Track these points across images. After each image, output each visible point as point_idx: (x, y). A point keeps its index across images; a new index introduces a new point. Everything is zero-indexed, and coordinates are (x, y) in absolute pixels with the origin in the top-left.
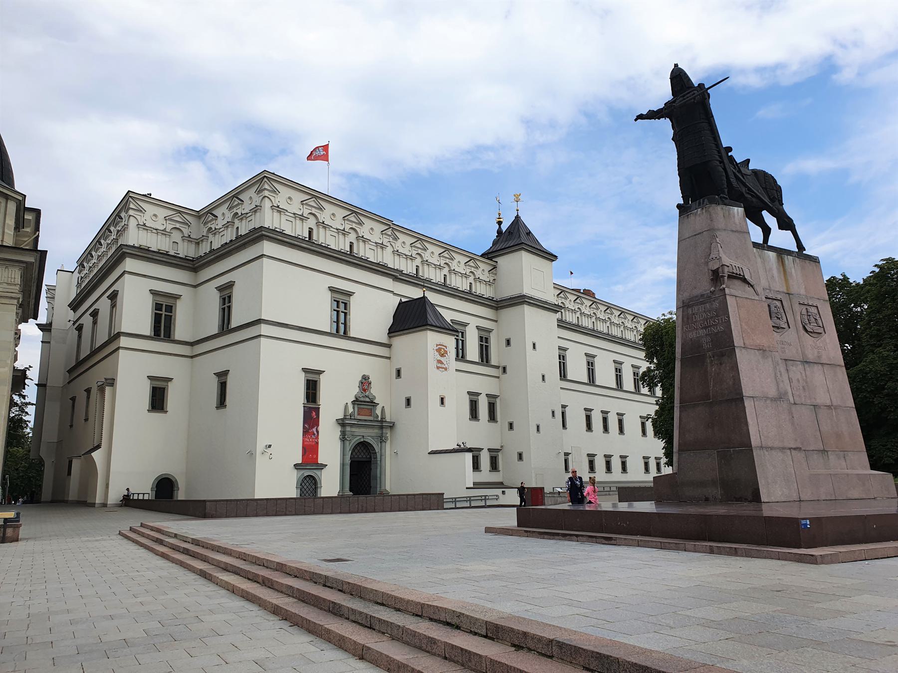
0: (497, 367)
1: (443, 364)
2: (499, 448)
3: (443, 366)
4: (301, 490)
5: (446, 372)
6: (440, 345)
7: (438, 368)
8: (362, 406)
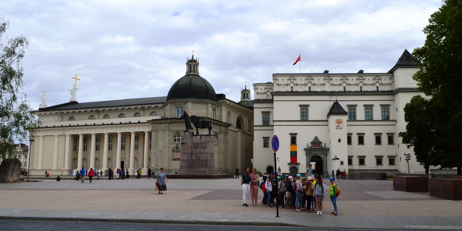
0: (395, 121)
1: (340, 126)
2: (396, 155)
3: (340, 127)
4: (291, 171)
5: (341, 130)
6: (338, 120)
7: (337, 128)
8: (315, 144)
